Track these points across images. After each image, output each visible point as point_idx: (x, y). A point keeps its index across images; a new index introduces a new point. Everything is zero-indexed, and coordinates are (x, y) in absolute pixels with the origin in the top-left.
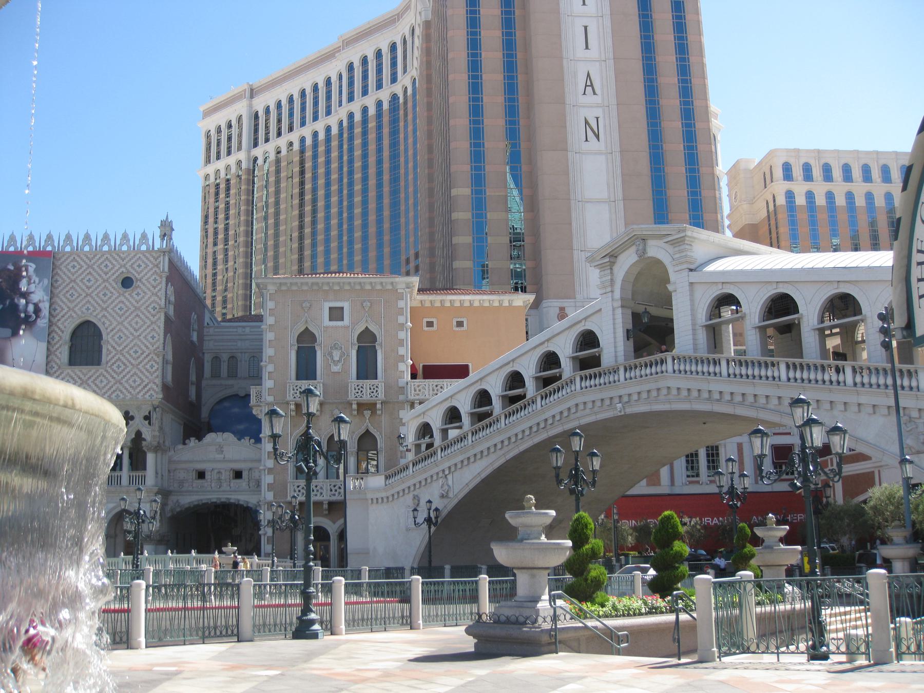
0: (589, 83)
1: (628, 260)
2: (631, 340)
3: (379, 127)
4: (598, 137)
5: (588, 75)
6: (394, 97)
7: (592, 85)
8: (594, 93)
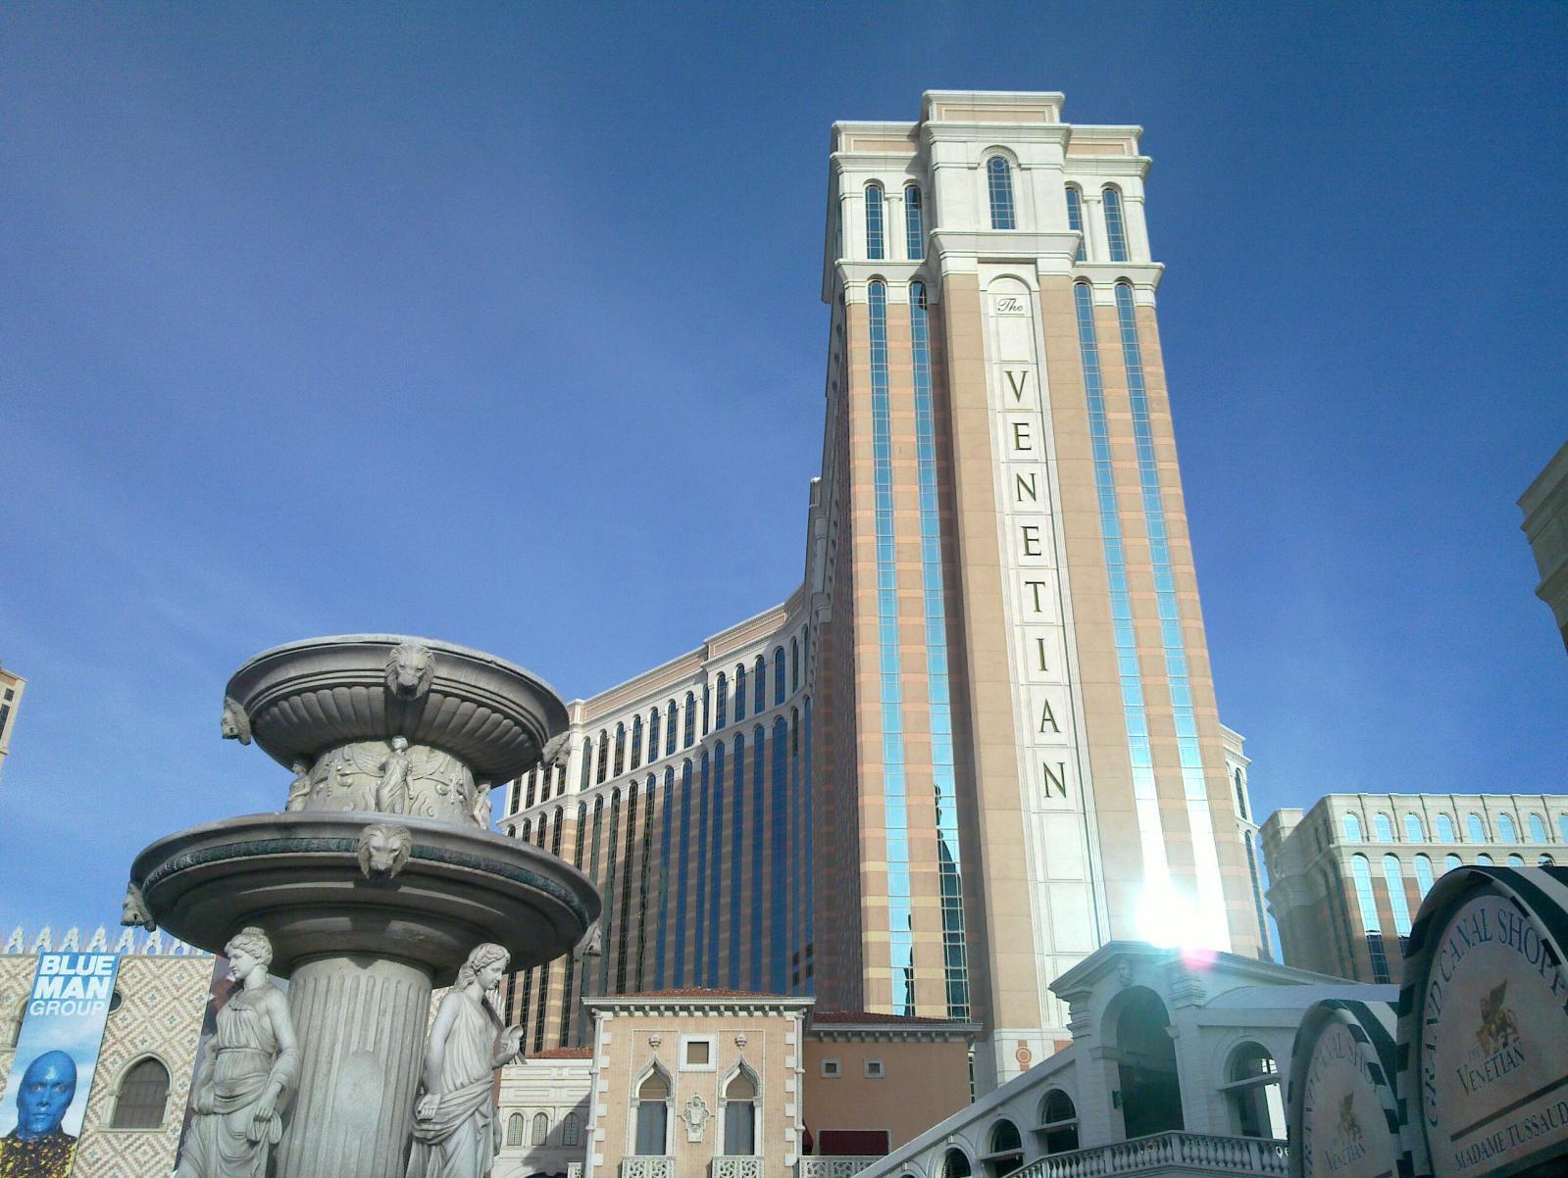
0: (1047, 716)
1: (1105, 992)
2: (1121, 1107)
3: (759, 764)
4: (1063, 790)
5: (1047, 703)
7: (1052, 719)
8: (1057, 731)
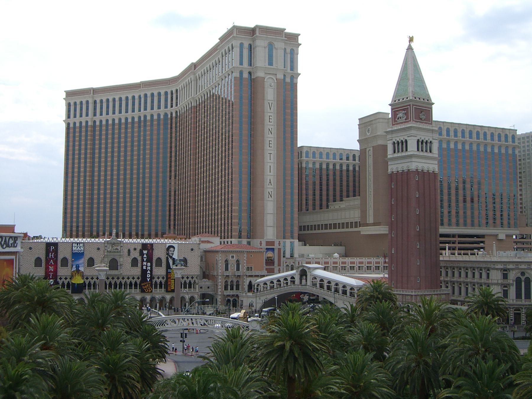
3: (159, 125)
6: (166, 115)
